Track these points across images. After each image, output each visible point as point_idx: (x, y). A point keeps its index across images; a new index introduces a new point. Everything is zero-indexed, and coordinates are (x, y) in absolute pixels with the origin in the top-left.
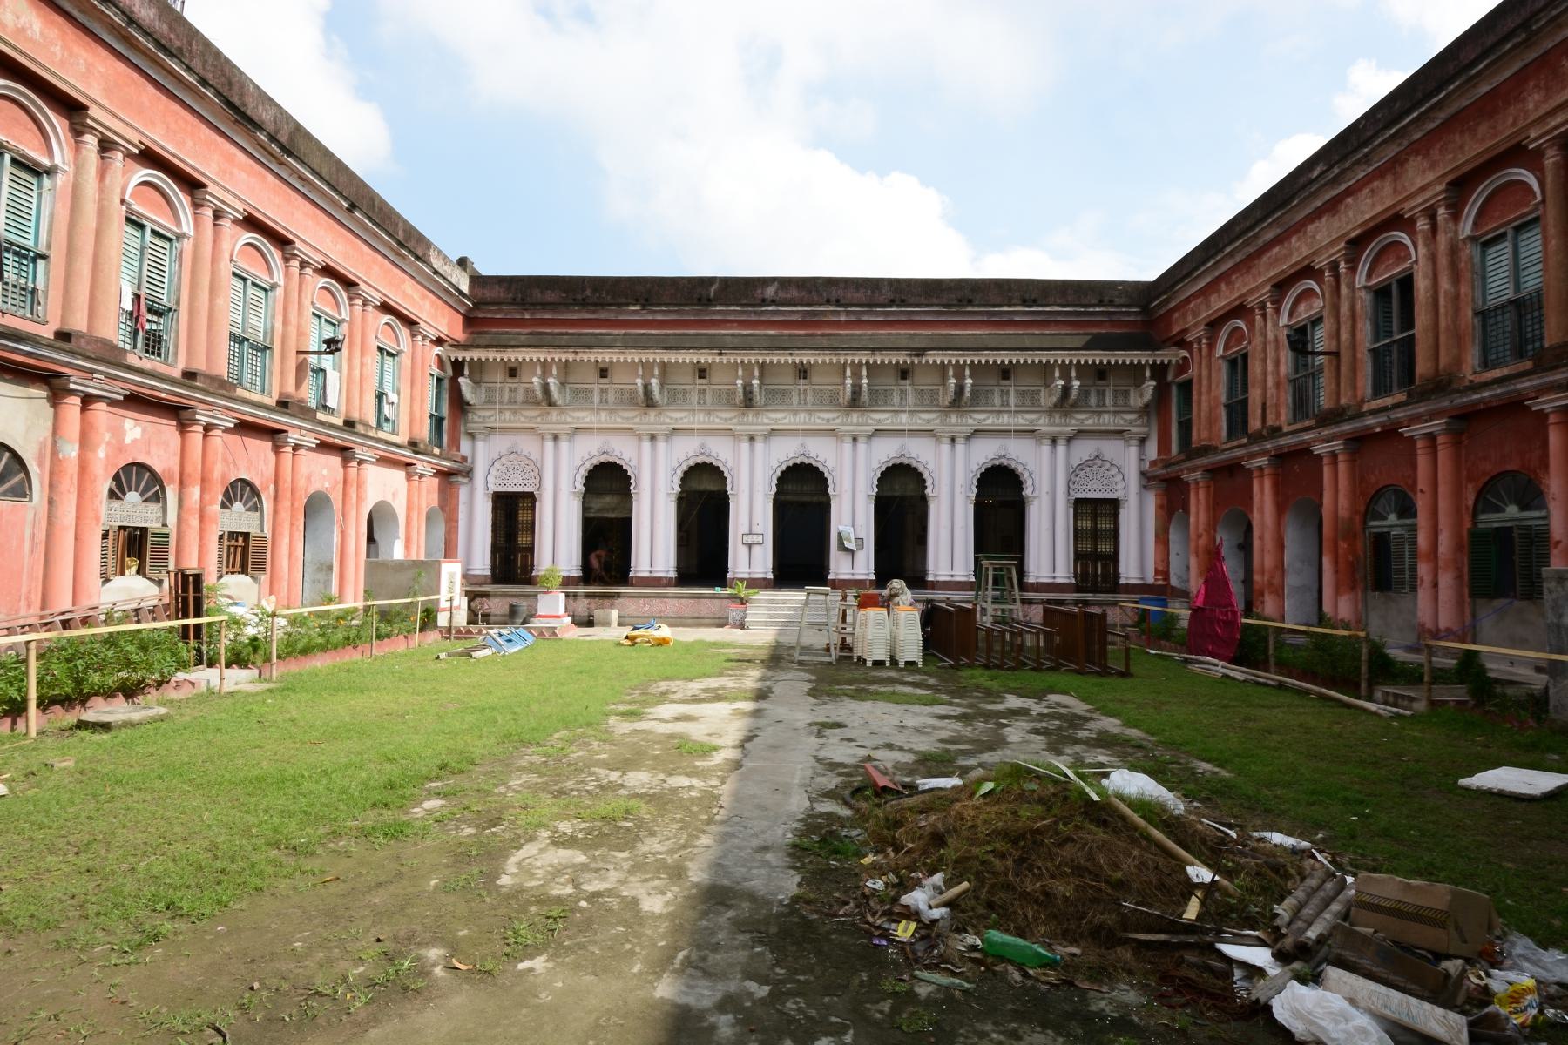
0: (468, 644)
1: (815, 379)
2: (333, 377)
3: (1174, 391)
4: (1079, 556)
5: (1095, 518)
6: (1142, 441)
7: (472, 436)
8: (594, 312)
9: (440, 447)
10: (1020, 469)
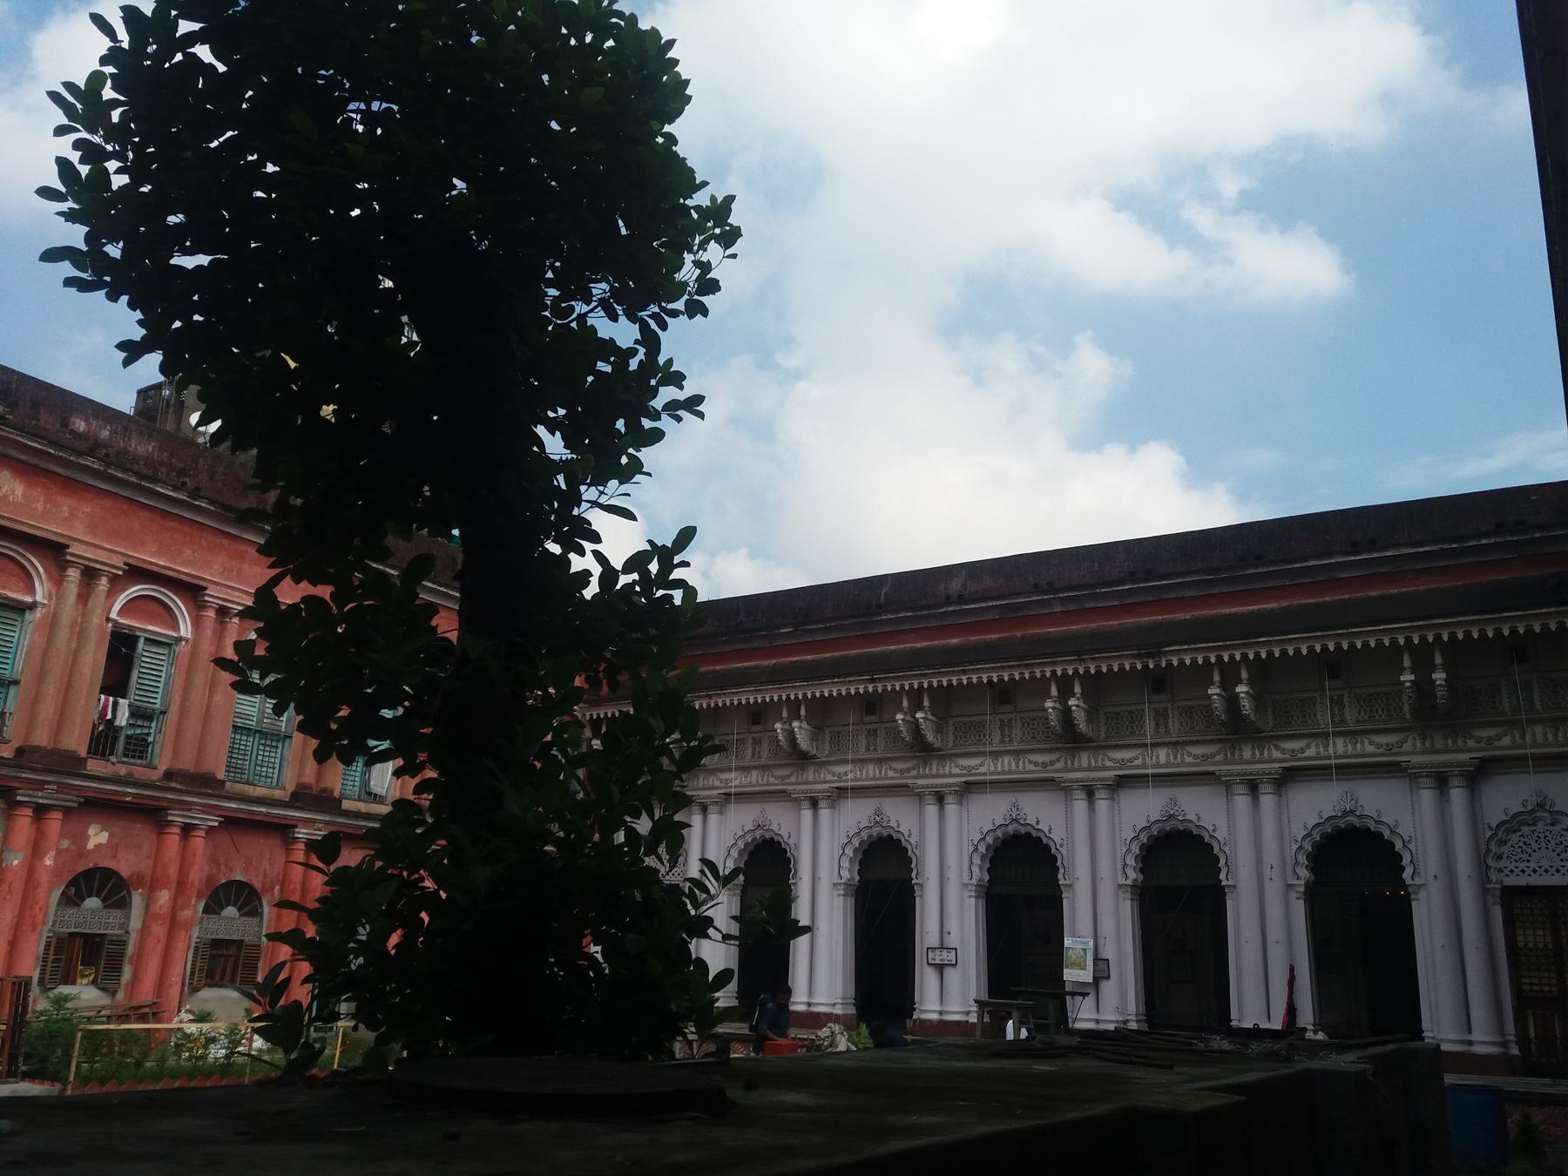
4: (1523, 1003)
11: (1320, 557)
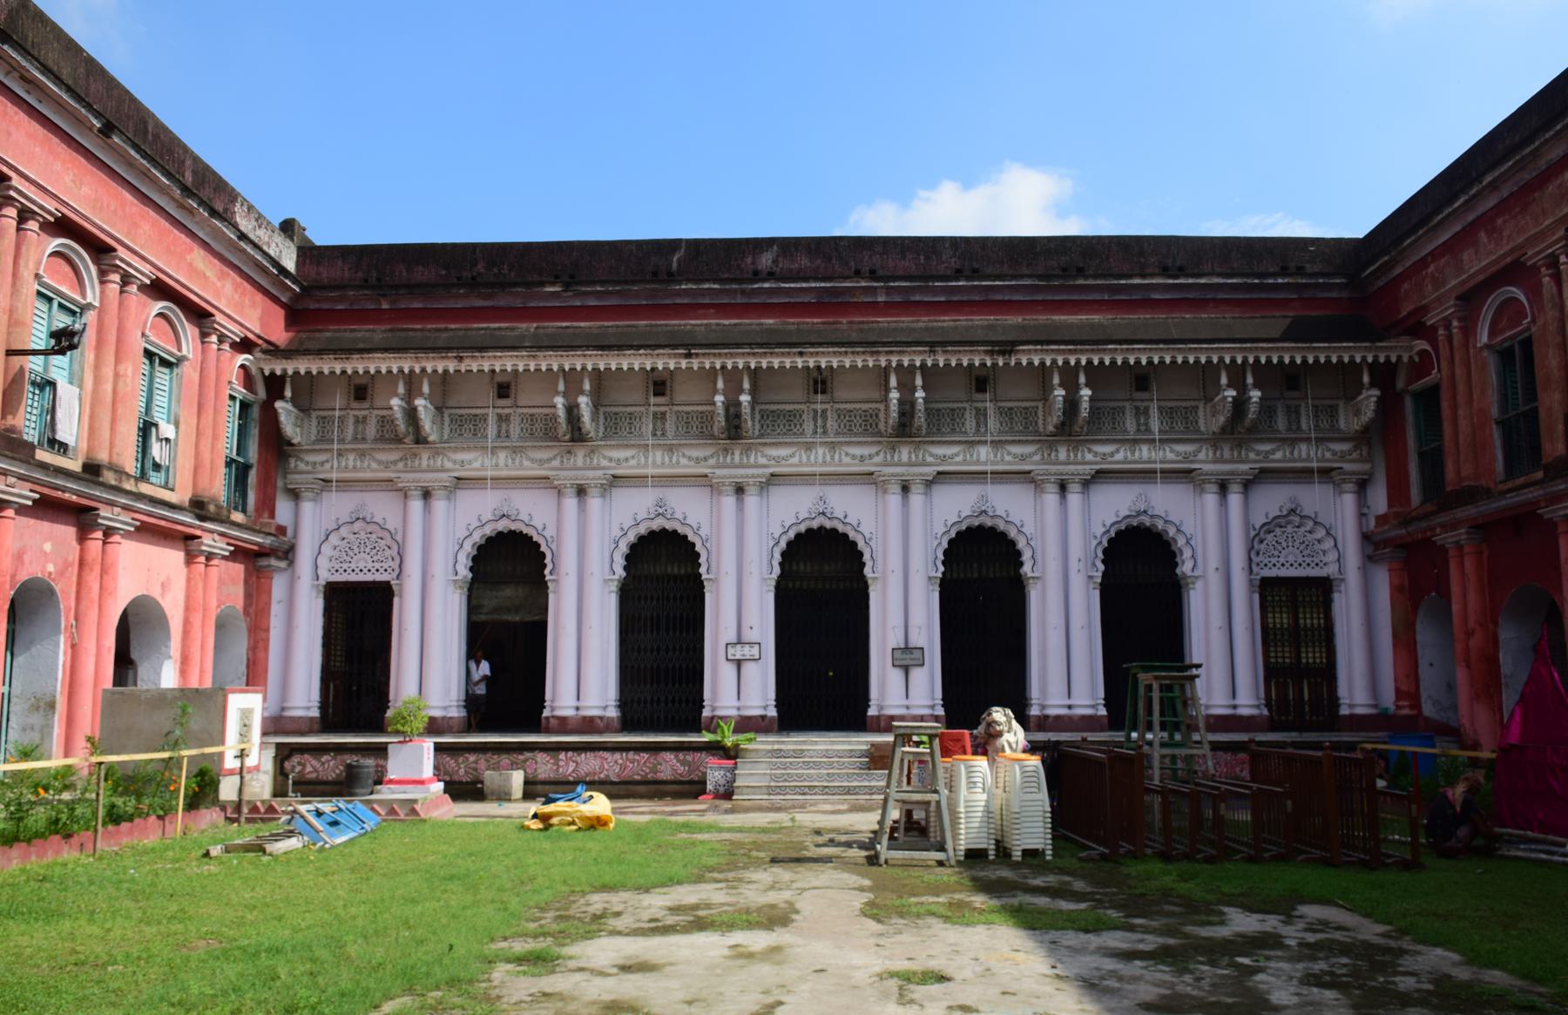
0: (265, 830)
1: (840, 394)
2: (68, 395)
3: (1409, 404)
5: (1293, 613)
6: (1362, 486)
7: (295, 495)
8: (489, 297)
9: (244, 511)
10: (1172, 532)
11: (1143, 276)
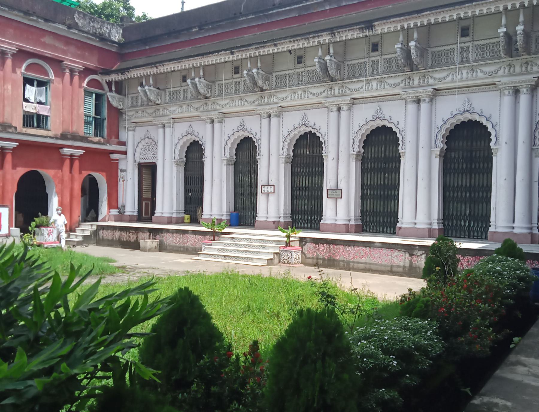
8: (177, 38)
